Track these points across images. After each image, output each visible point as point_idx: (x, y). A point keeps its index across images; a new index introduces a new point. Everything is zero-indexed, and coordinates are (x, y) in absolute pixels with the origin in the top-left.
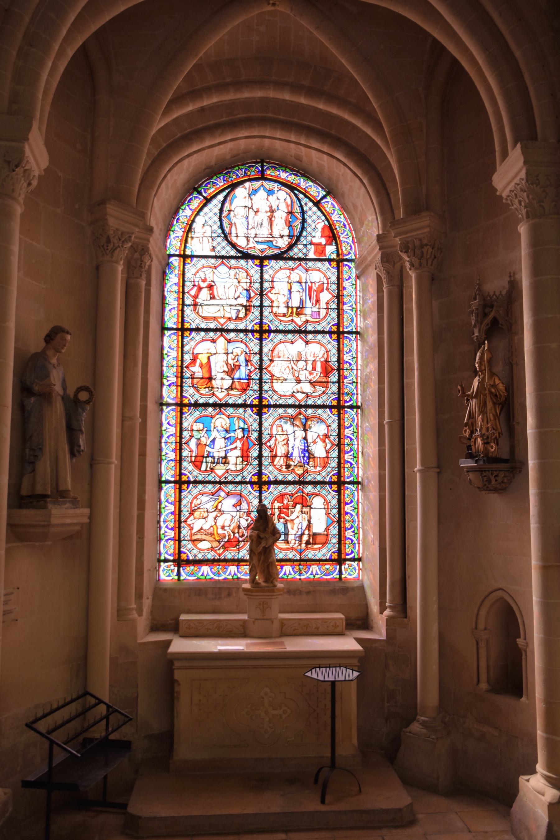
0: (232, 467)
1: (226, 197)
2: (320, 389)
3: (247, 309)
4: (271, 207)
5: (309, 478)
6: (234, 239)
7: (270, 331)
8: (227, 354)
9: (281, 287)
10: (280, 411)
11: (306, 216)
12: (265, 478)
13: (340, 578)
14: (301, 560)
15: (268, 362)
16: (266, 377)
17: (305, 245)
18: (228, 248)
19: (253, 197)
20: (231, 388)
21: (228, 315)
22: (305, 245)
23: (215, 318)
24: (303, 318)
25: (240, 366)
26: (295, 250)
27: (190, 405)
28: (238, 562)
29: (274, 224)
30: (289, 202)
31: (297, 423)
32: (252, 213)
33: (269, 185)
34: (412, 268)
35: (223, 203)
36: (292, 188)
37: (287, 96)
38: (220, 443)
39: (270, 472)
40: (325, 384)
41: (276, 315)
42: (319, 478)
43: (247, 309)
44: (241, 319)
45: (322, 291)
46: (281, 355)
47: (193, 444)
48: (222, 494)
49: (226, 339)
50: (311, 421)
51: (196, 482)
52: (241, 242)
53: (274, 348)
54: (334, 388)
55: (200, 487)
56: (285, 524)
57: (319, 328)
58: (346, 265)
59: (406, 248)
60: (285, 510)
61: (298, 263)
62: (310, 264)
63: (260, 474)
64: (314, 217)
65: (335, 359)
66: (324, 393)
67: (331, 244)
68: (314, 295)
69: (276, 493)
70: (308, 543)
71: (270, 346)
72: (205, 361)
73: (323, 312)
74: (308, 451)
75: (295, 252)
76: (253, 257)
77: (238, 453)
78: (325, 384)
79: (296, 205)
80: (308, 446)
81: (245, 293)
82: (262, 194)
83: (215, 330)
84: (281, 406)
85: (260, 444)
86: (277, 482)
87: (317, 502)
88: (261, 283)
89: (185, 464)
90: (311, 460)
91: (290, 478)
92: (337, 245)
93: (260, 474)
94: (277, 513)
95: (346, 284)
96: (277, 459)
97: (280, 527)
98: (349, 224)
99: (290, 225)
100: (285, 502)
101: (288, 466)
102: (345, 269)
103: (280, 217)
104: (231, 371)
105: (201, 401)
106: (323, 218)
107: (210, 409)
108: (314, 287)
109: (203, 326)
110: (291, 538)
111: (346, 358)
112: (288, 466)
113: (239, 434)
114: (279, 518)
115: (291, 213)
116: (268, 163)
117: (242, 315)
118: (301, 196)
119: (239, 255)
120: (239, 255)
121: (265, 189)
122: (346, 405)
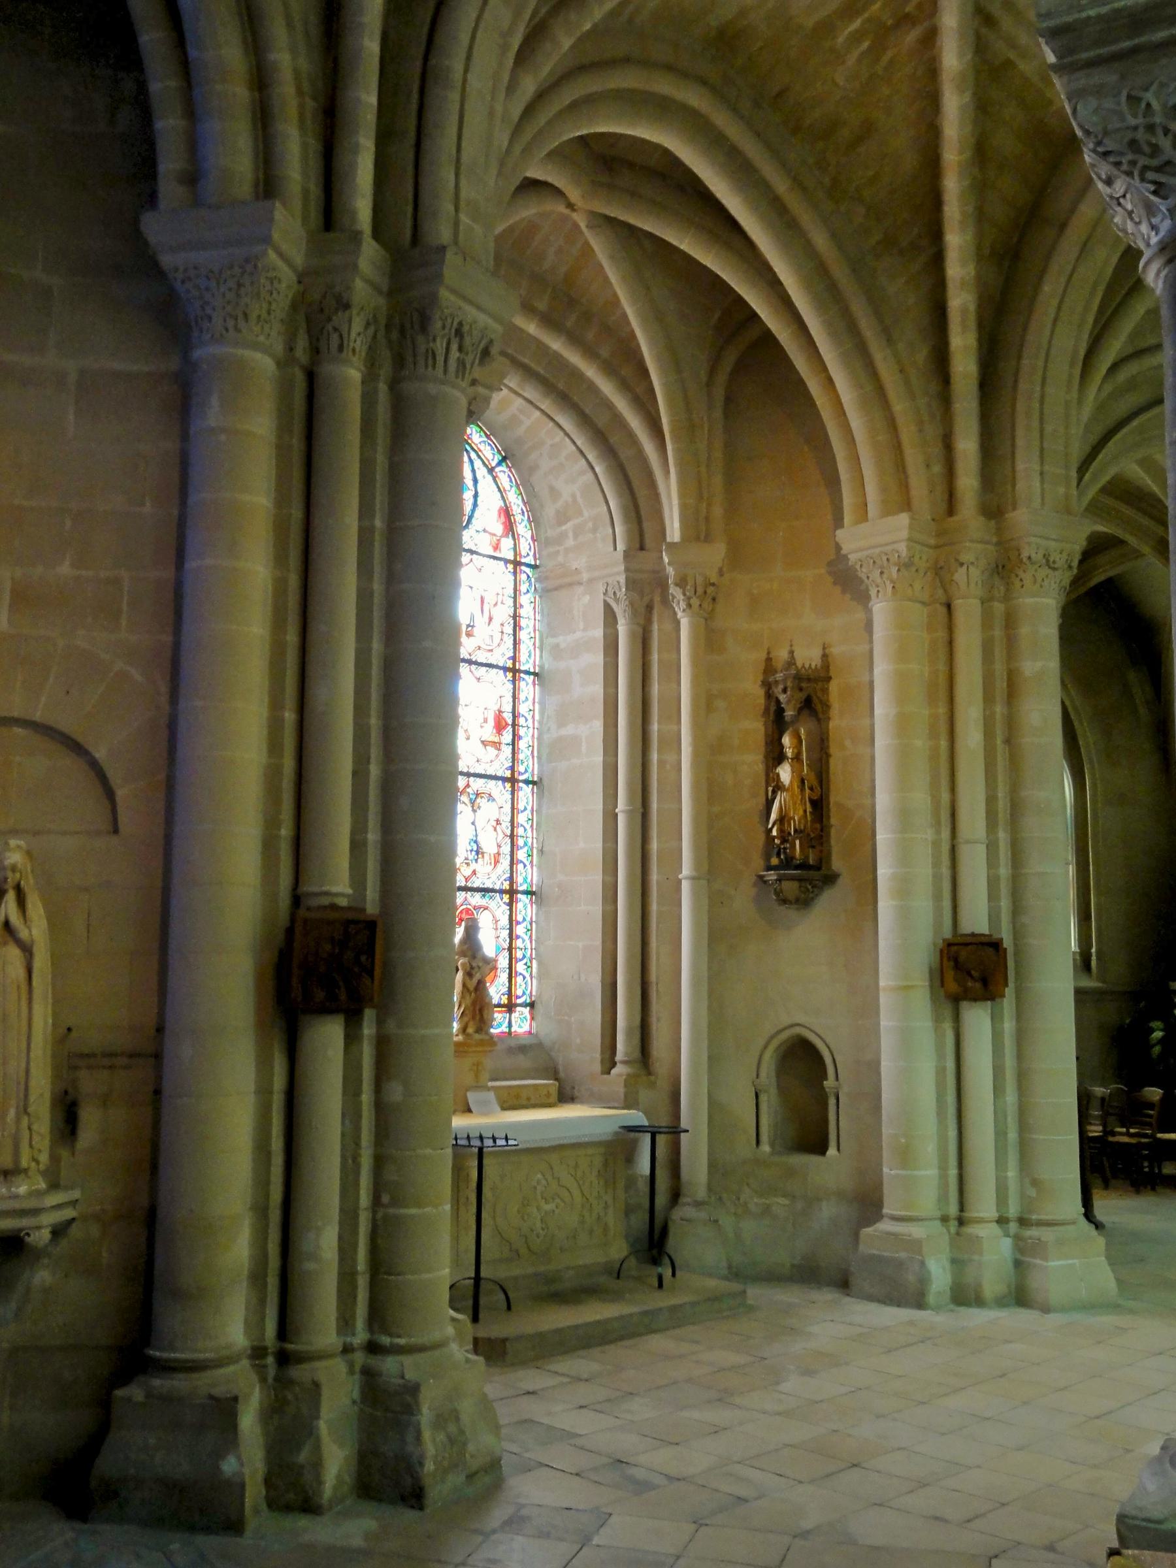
5: (477, 883)
13: (510, 1033)
34: (688, 610)
40: (497, 745)
42: (489, 885)
45: (496, 605)
50: (482, 797)
54: (507, 751)
58: (525, 572)
59: (681, 583)
65: (510, 709)
67: (506, 535)
74: (476, 842)
80: (476, 836)
90: (480, 856)
98: (527, 511)
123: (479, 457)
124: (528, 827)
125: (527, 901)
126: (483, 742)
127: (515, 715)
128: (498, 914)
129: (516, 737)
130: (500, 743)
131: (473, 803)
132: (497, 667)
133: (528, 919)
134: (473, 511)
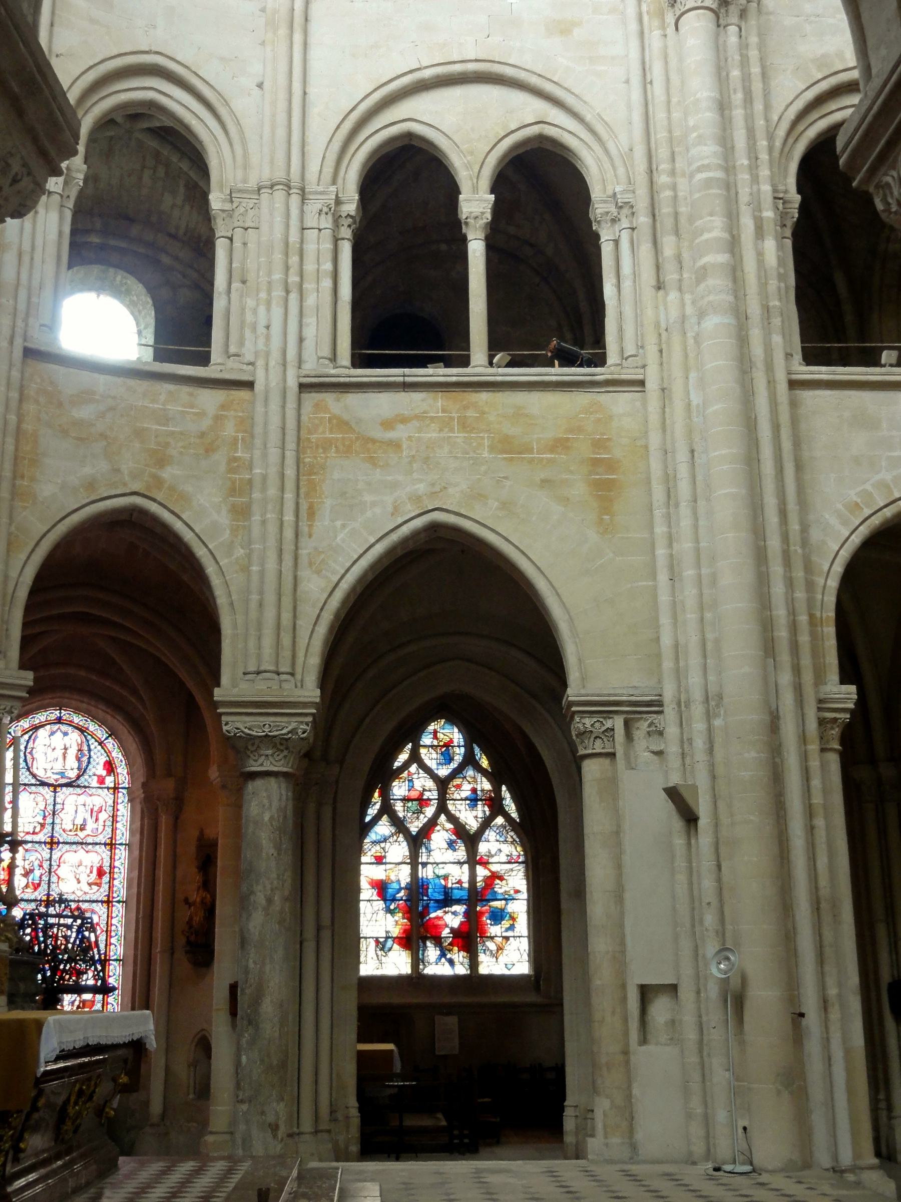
1: (30, 737)
2: (95, 888)
3: (43, 826)
4: (65, 746)
6: (35, 771)
7: (58, 843)
8: (24, 860)
9: (69, 808)
11: (92, 753)
15: (56, 867)
16: (54, 879)
17: (90, 776)
18: (30, 777)
19: (51, 737)
20: (27, 886)
21: (27, 830)
22: (90, 776)
24: (85, 833)
25: (34, 869)
26: (82, 779)
29: (67, 758)
30: (80, 742)
32: (50, 750)
33: (64, 728)
35: (28, 742)
36: (82, 730)
37: (82, 673)
40: (99, 885)
41: (64, 831)
43: (43, 826)
44: (37, 833)
45: (101, 811)
46: (66, 861)
49: (24, 849)
52: (40, 773)
53: (61, 856)
57: (97, 840)
61: (83, 790)
64: (99, 754)
66: (98, 890)
68: (94, 814)
71: (59, 854)
73: (100, 830)
75: (82, 781)
76: (49, 785)
78: (99, 885)
81: (42, 812)
82: (59, 734)
92: (114, 776)
95: (120, 807)
99: (78, 759)
103: (72, 753)
104: (26, 874)
106: (105, 755)
111: (117, 864)
115: (79, 750)
116: (65, 710)
117: (37, 830)
118: (89, 737)
119: (38, 783)
120: (38, 783)
121: (61, 731)
122: (114, 900)
123: (93, 737)
124: (119, 925)
125: (116, 965)
126: (88, 884)
127: (112, 867)
129: (112, 879)
130: (101, 883)
132: (100, 844)
133: (117, 974)
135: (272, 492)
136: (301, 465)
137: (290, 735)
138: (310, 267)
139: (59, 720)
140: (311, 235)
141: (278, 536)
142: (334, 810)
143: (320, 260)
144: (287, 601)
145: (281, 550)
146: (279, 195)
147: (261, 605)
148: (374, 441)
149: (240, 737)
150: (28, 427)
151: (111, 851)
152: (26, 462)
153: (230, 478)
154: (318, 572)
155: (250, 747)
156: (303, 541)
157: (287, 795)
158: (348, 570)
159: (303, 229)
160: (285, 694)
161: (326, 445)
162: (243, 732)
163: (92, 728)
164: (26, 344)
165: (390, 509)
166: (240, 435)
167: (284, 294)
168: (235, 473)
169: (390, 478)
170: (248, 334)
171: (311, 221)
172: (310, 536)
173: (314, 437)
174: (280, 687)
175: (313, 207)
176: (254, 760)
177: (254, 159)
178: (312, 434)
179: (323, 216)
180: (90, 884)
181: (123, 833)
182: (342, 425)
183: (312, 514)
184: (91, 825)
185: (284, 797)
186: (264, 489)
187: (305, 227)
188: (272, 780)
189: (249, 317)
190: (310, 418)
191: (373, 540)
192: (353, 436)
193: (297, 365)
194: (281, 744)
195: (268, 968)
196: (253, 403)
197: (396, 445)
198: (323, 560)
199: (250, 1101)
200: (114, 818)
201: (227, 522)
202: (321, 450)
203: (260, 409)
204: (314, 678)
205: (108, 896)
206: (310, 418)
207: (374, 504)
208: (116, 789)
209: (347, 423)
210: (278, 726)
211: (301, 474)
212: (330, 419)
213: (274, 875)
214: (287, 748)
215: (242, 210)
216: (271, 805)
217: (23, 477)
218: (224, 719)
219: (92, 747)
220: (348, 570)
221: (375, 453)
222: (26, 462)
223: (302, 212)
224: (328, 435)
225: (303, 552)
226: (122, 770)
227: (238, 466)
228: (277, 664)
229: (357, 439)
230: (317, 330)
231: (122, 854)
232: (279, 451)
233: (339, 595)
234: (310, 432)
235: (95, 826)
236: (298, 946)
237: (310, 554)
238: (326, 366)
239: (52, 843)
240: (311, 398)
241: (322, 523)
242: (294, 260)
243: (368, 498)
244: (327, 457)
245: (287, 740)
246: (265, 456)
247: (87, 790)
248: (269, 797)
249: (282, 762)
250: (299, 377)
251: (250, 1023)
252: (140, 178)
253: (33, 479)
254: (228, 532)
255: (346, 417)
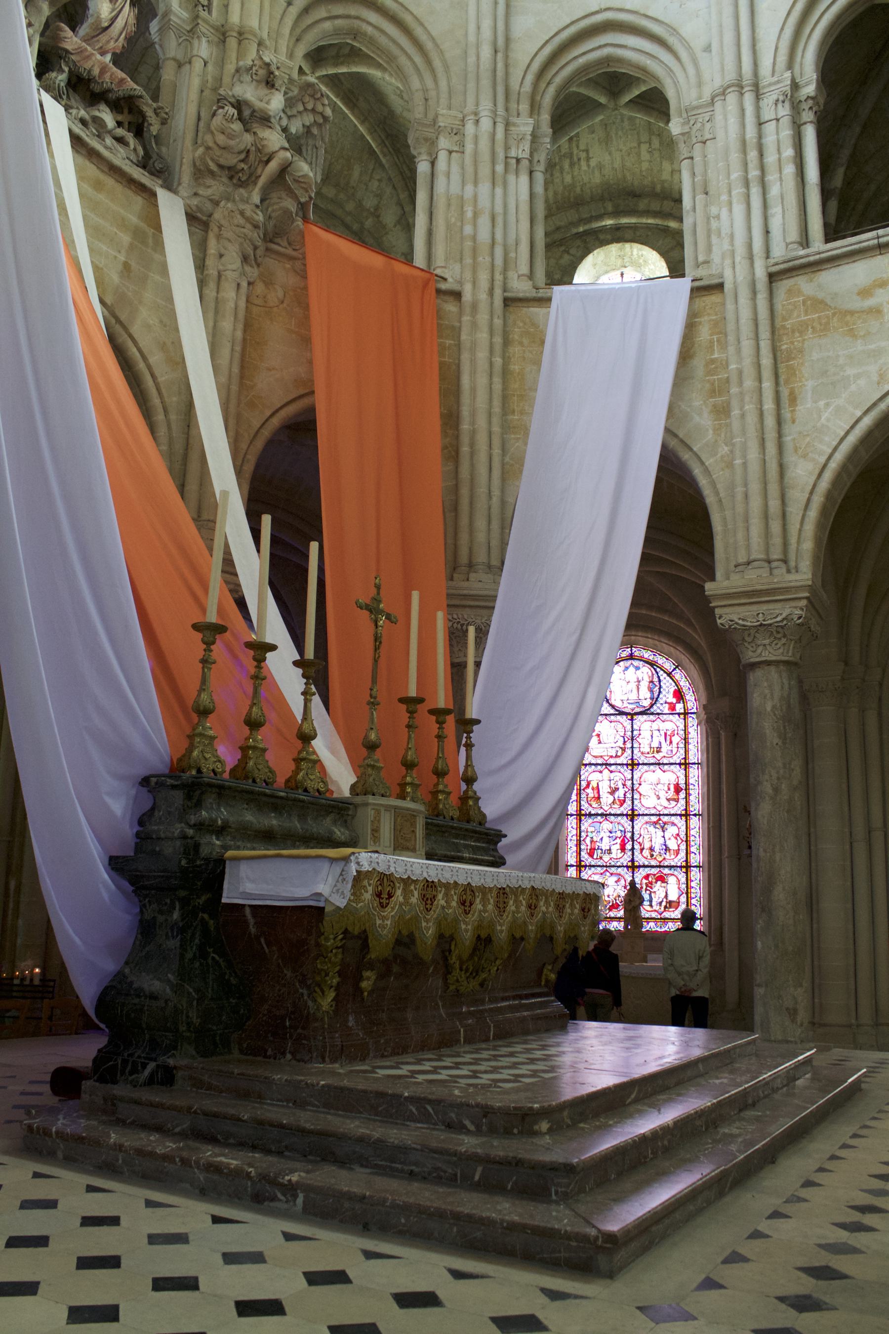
0: (613, 855)
2: (674, 803)
3: (624, 750)
5: (666, 864)
6: (613, 702)
7: (638, 764)
9: (646, 734)
10: (646, 818)
12: (636, 864)
14: (661, 919)
16: (636, 796)
23: (601, 757)
24: (661, 755)
26: (655, 707)
27: (585, 815)
28: (618, 919)
31: (658, 826)
33: (636, 663)
36: (652, 664)
38: (606, 840)
39: (639, 859)
41: (642, 753)
42: (673, 864)
43: (624, 750)
47: (588, 841)
48: (608, 874)
51: (591, 866)
52: (618, 704)
55: (593, 869)
56: (650, 895)
57: (672, 761)
60: (650, 885)
62: (665, 716)
63: (633, 861)
65: (684, 782)
69: (644, 874)
70: (665, 907)
72: (595, 786)
73: (675, 750)
75: (655, 709)
76: (626, 714)
77: (618, 846)
78: (677, 800)
79: (655, 676)
82: (632, 669)
83: (602, 765)
84: (646, 815)
85: (633, 840)
86: (644, 866)
87: (672, 880)
88: (632, 732)
89: (583, 854)
91: (653, 863)
93: (633, 861)
94: (644, 887)
95: (690, 730)
96: (644, 851)
97: (646, 896)
100: (650, 879)
101: (652, 856)
102: (690, 719)
103: (644, 685)
104: (613, 792)
105: (593, 812)
107: (599, 818)
108: (669, 733)
109: (593, 762)
110: (654, 903)
111: (691, 781)
112: (652, 856)
113: (619, 834)
114: (646, 890)
115: (652, 682)
117: (619, 754)
118: (658, 670)
124: (697, 836)
127: (687, 783)
128: (680, 877)
129: (688, 795)
131: (662, 828)
134: (659, 695)
135: (749, 383)
136: (779, 354)
137: (785, 622)
138: (771, 158)
139: (631, 657)
140: (770, 128)
141: (758, 426)
142: (880, 714)
143: (781, 150)
144: (773, 489)
145: (763, 439)
146: (732, 98)
147: (746, 496)
148: (852, 313)
149: (735, 628)
150: (515, 367)
151: (685, 770)
152: (516, 398)
153: (709, 381)
154: (804, 456)
155: (747, 638)
156: (787, 428)
157: (789, 684)
158: (835, 449)
159: (760, 124)
160: (775, 580)
161: (802, 328)
162: (737, 623)
163: (660, 662)
164: (506, 294)
165: (875, 378)
166: (715, 337)
167: (744, 190)
168: (712, 375)
169: (872, 347)
170: (714, 240)
171: (768, 113)
172: (794, 422)
173: (788, 324)
174: (771, 574)
175: (768, 102)
176: (754, 652)
177: (706, 76)
178: (787, 320)
179: (780, 105)
180: (668, 800)
181: (695, 754)
182: (817, 304)
183: (793, 399)
184: (665, 748)
185: (786, 686)
186: (740, 383)
187: (762, 121)
188: (773, 669)
189: (714, 224)
190: (783, 306)
191: (859, 413)
192: (830, 313)
193: (764, 255)
194: (778, 632)
195: (778, 856)
196: (723, 304)
197: (877, 311)
198: (809, 443)
199: (767, 986)
200: (686, 740)
201: (709, 423)
202: (797, 334)
203: (730, 306)
204: (808, 563)
205: (686, 810)
206: (783, 306)
207: (858, 376)
208: (686, 714)
209: (822, 302)
210: (772, 614)
211: (779, 362)
212: (804, 302)
213: (780, 764)
214: (785, 636)
215: (699, 125)
216: (772, 695)
217: (513, 412)
218: (718, 611)
219: (662, 678)
220: (835, 449)
221: (854, 324)
222: (516, 398)
223: (758, 109)
224: (803, 318)
225: (788, 439)
226: (690, 697)
227: (716, 368)
228: (767, 554)
229: (834, 314)
230: (783, 218)
231: (695, 774)
232: (752, 342)
233: (828, 476)
234: (784, 319)
235: (670, 748)
236: (848, 847)
237: (794, 439)
238: (795, 249)
239: (633, 765)
240: (783, 286)
241: (805, 406)
242: (753, 155)
243: (850, 371)
244: (804, 340)
245: (782, 627)
246: (739, 351)
247: (660, 716)
248: (770, 687)
249: (781, 651)
250: (767, 267)
251: (763, 910)
252: (639, 155)
253: (522, 412)
254: (711, 432)
255: (820, 295)
